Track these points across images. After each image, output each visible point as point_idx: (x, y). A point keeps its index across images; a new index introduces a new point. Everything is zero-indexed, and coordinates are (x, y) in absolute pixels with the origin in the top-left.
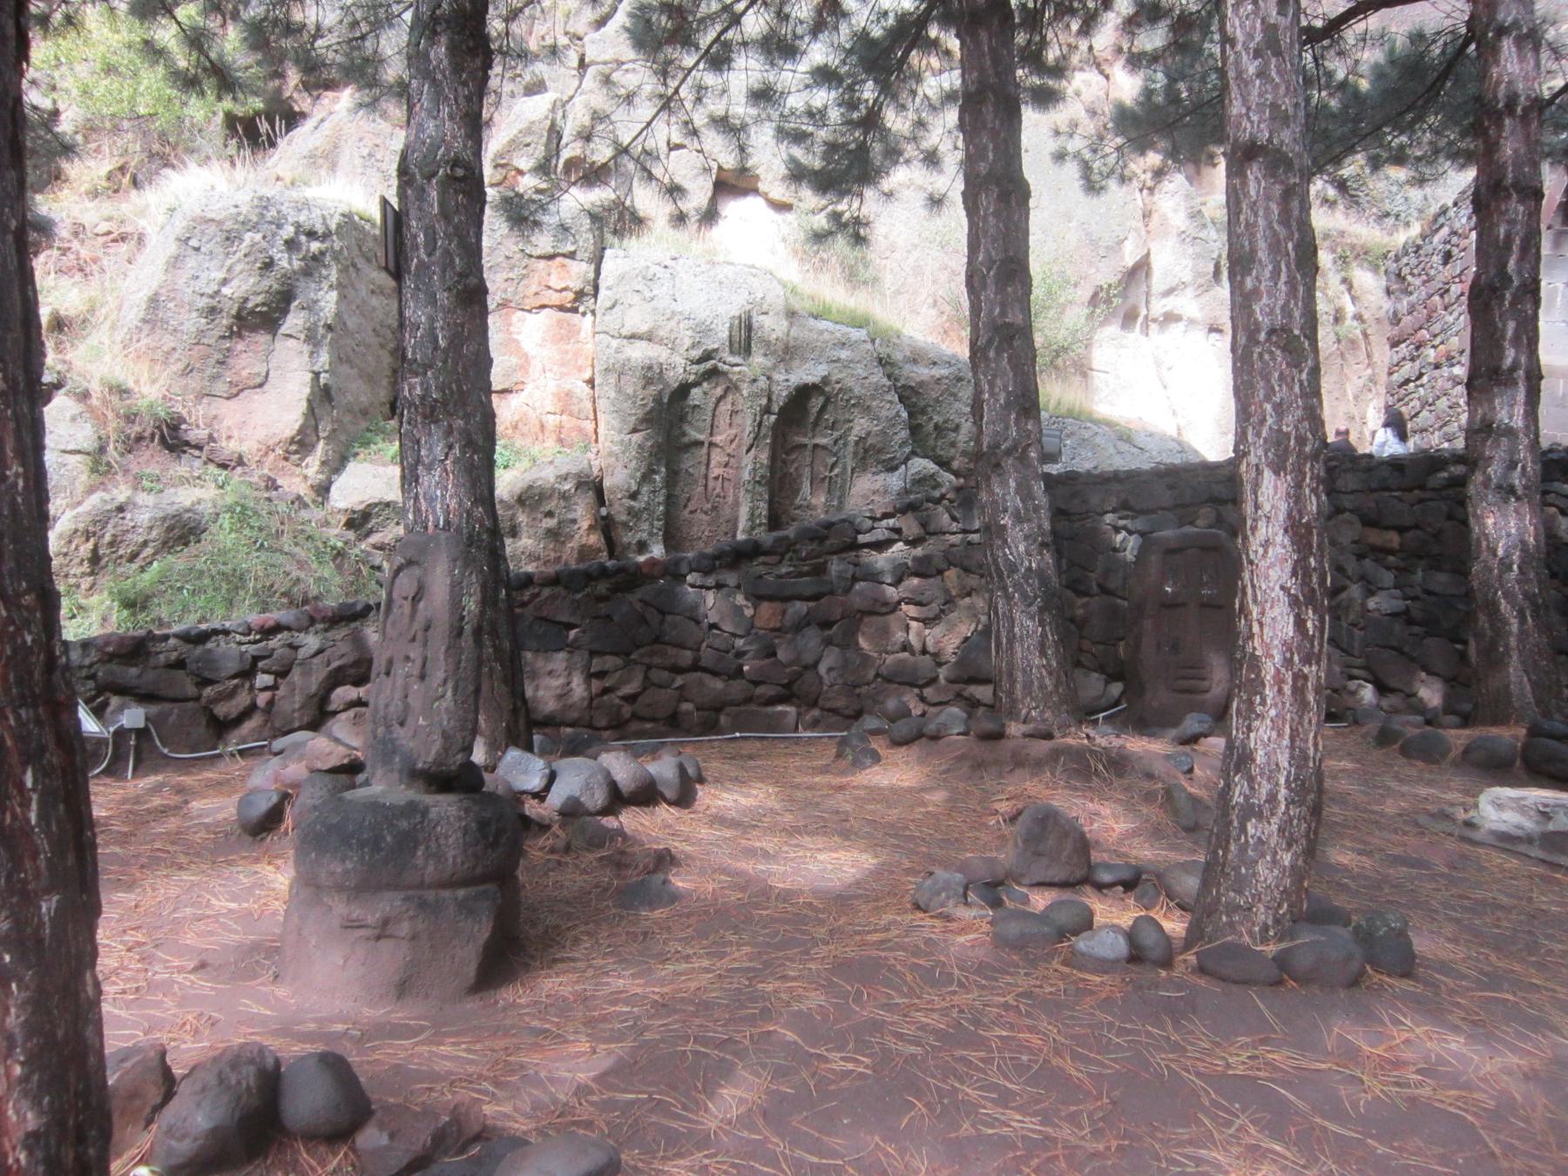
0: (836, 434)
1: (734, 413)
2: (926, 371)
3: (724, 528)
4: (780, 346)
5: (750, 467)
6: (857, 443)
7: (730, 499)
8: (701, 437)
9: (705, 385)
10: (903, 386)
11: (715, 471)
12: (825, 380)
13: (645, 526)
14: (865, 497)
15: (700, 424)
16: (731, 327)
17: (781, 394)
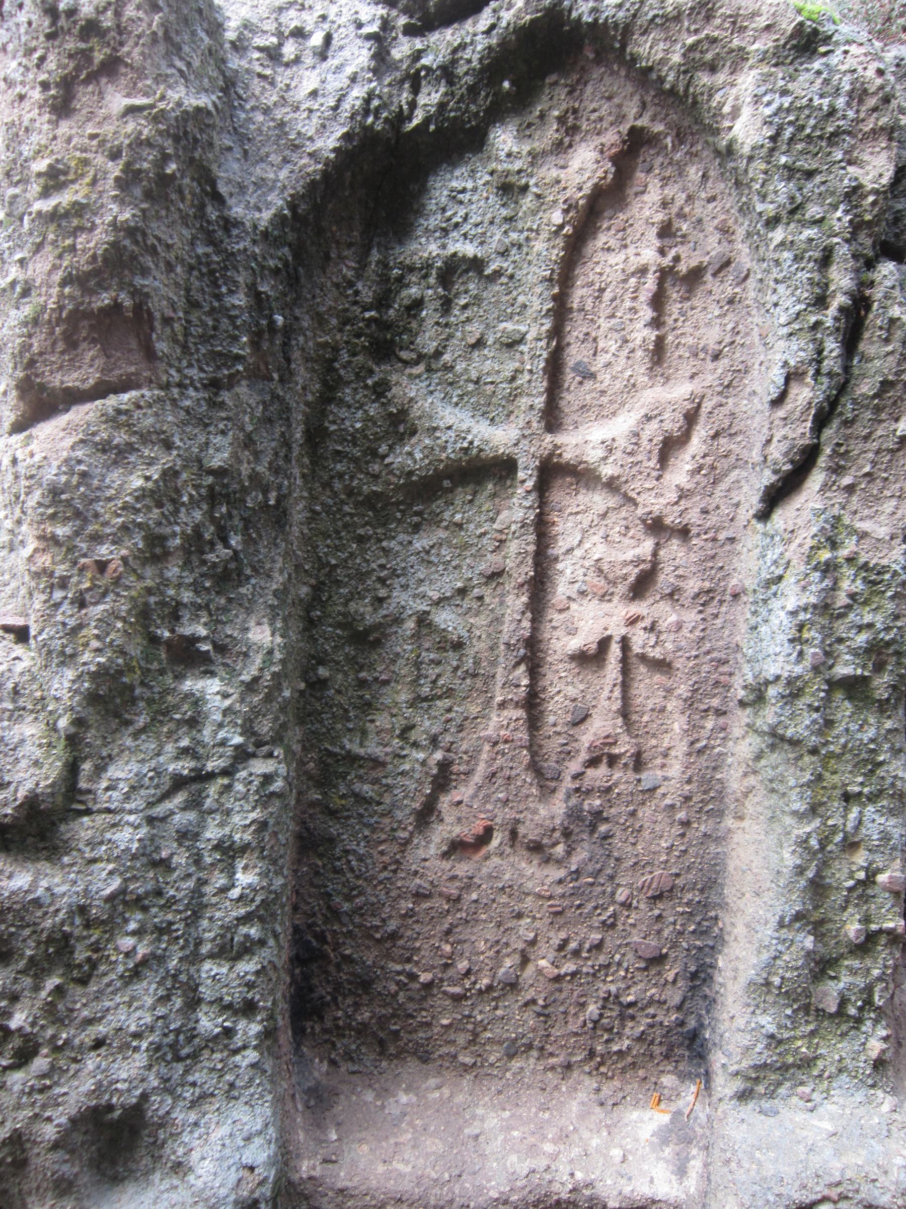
1: (676, 283)
3: (637, 933)
5: (792, 597)
7: (671, 773)
8: (498, 437)
9: (504, 138)
11: (583, 619)
13: (133, 1010)
15: (486, 364)
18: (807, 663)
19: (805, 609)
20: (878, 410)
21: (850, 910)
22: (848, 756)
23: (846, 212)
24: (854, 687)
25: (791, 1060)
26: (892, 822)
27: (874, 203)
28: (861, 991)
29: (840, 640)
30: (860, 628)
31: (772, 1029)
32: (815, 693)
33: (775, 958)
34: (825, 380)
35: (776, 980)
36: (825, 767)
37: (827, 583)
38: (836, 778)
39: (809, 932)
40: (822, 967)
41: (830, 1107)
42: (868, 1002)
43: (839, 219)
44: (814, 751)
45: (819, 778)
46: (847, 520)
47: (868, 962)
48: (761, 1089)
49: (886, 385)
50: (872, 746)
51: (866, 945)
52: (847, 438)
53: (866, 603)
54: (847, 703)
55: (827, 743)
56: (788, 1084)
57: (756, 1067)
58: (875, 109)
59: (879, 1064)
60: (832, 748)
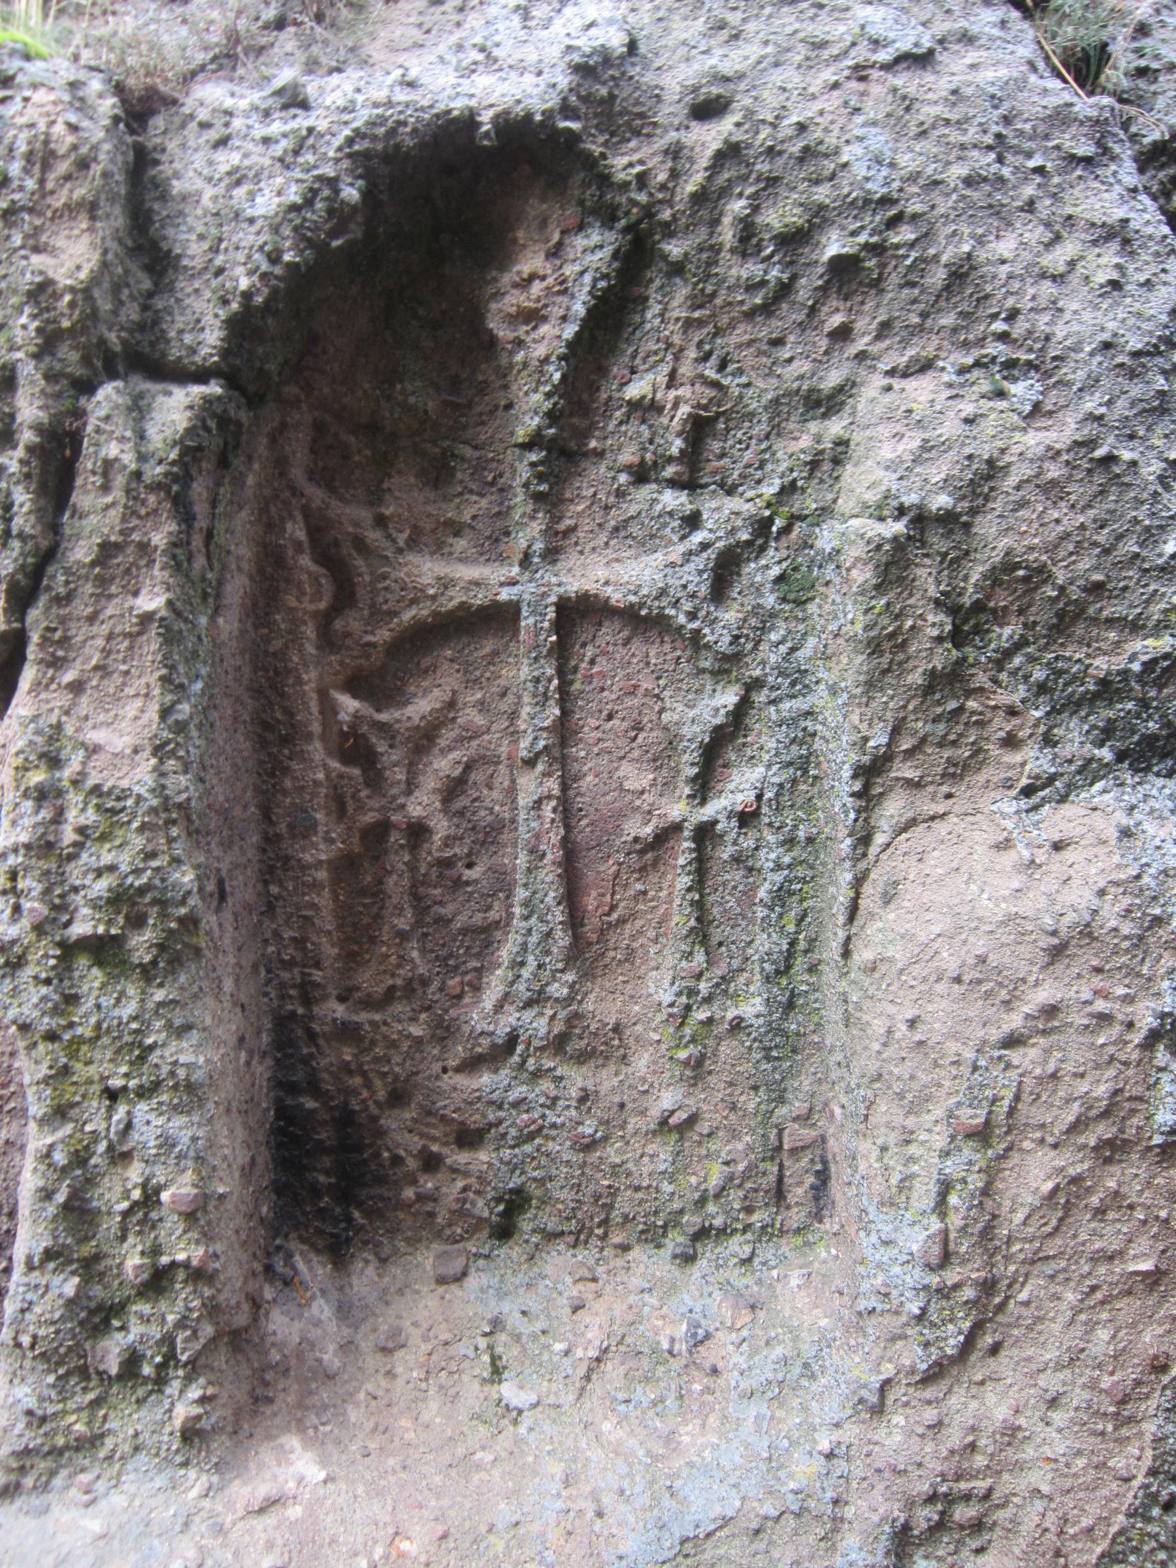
0: (726, 516)
6: (893, 566)
12: (605, 87)
14: (983, 981)
17: (247, 189)
18: (25, 923)
19: (15, 851)
20: (103, 582)
21: (131, 1240)
22: (105, 1040)
23: (34, 317)
24: (104, 950)
25: (60, 1441)
26: (179, 1121)
27: (72, 305)
28: (160, 1343)
29: (76, 890)
30: (99, 873)
31: (31, 1403)
32: (42, 958)
33: (23, 1311)
34: (16, 544)
35: (26, 1340)
36: (73, 1054)
37: (45, 814)
38: (92, 1070)
39: (73, 1273)
40: (99, 1317)
41: (118, 1500)
42: (170, 1357)
43: (24, 327)
44: (51, 1037)
45: (66, 1071)
46: (69, 730)
47: (163, 1305)
48: (29, 1482)
49: (107, 550)
50: (134, 1026)
51: (158, 1281)
52: (63, 620)
53: (104, 838)
54: (95, 971)
55: (71, 1025)
56: (64, 1473)
57: (17, 1455)
58: (68, 178)
59: (191, 1434)
60: (79, 1031)
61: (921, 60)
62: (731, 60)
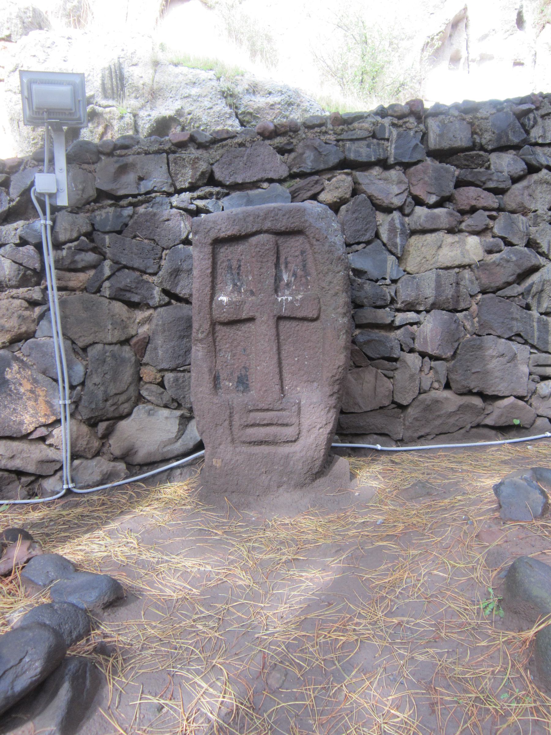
2: (263, 99)
4: (147, 89)
10: (243, 113)
12: (179, 113)
16: (103, 77)
61: (211, 108)
62: (191, 108)
